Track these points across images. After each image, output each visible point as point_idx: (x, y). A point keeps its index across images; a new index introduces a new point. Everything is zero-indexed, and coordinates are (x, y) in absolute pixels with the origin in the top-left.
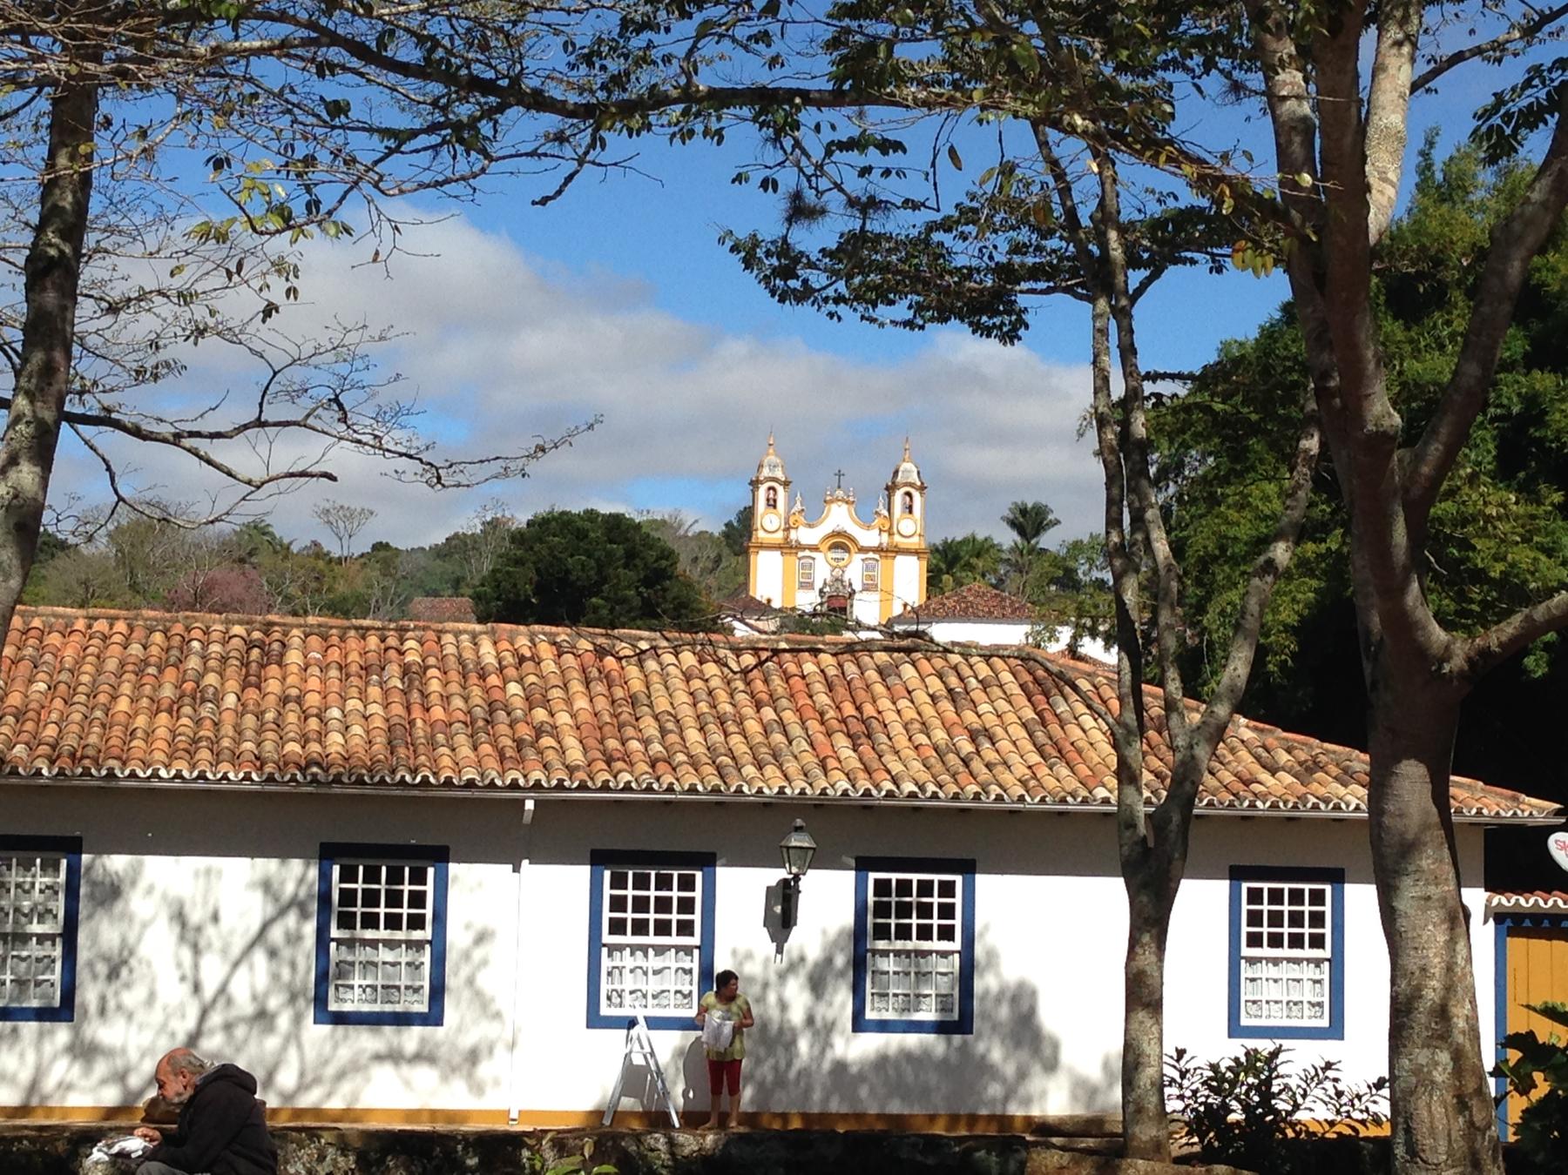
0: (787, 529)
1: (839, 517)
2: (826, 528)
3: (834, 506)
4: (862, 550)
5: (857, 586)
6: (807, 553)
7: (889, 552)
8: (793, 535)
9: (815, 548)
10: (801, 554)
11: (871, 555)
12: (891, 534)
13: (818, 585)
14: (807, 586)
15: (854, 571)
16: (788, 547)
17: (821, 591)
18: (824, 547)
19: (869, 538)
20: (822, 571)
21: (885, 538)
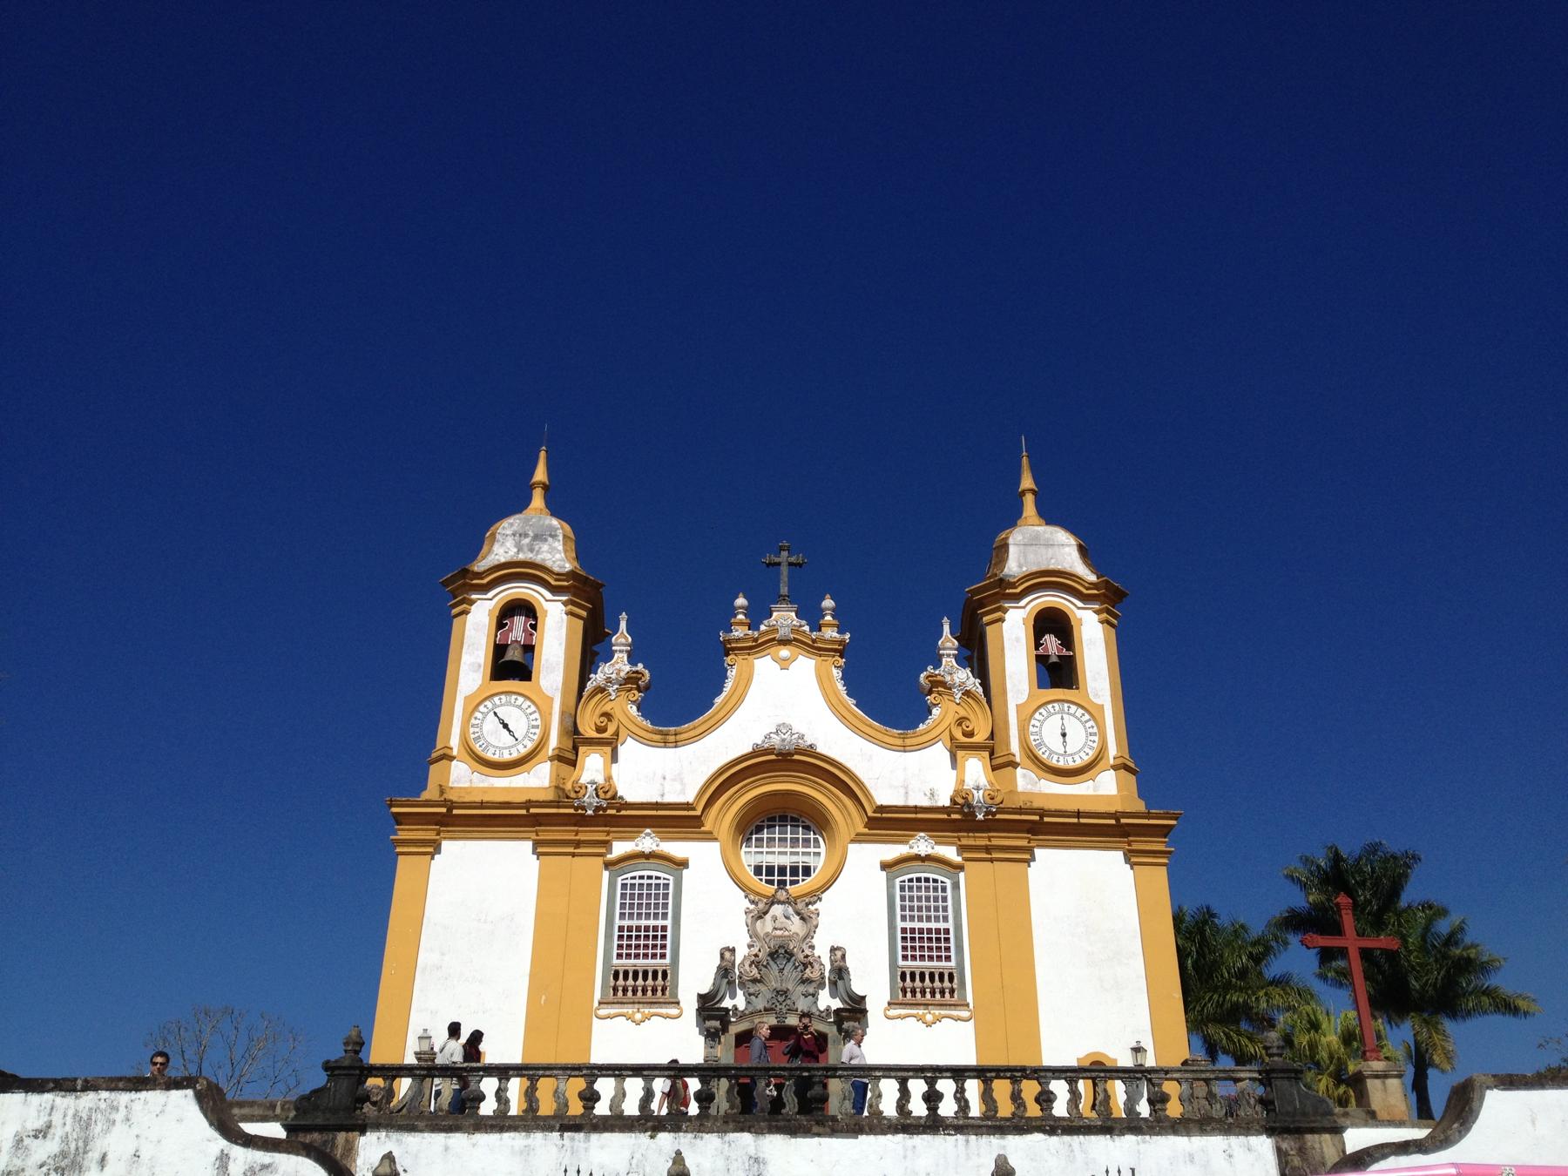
0: (567, 759)
1: (785, 694)
2: (735, 733)
3: (764, 666)
4: (889, 822)
5: (872, 979)
6: (648, 842)
7: (995, 829)
8: (592, 766)
9: (680, 820)
10: (620, 848)
11: (922, 845)
12: (1000, 763)
13: (696, 977)
14: (642, 983)
15: (855, 915)
16: (570, 823)
17: (708, 1007)
18: (723, 818)
19: (915, 773)
20: (713, 913)
21: (976, 771)
